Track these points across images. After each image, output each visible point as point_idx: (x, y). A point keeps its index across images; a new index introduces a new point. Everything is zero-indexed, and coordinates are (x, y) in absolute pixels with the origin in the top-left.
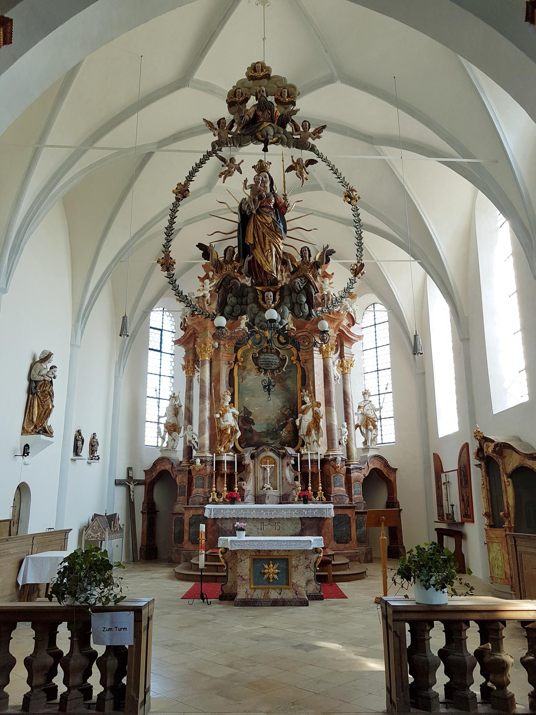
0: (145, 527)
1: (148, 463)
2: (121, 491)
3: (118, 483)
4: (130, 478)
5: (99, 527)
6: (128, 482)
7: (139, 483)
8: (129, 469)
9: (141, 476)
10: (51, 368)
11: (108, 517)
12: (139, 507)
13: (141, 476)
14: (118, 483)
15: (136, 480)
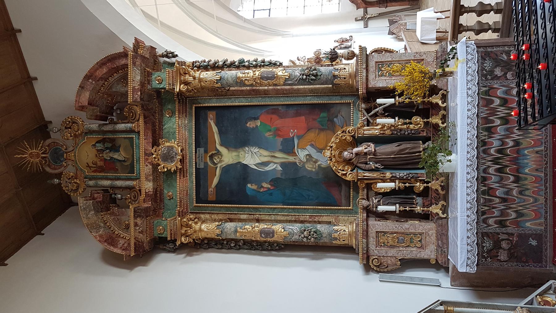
0: (397, 4)
1: (352, 7)
2: (371, 23)
3: (366, 26)
4: (362, 19)
5: (397, 28)
6: (365, 20)
7: (366, 12)
8: (356, 20)
9: (361, 11)
10: (299, 60)
11: (390, 25)
12: (383, 10)
13: (361, 11)
14: (366, 26)
15: (364, 14)
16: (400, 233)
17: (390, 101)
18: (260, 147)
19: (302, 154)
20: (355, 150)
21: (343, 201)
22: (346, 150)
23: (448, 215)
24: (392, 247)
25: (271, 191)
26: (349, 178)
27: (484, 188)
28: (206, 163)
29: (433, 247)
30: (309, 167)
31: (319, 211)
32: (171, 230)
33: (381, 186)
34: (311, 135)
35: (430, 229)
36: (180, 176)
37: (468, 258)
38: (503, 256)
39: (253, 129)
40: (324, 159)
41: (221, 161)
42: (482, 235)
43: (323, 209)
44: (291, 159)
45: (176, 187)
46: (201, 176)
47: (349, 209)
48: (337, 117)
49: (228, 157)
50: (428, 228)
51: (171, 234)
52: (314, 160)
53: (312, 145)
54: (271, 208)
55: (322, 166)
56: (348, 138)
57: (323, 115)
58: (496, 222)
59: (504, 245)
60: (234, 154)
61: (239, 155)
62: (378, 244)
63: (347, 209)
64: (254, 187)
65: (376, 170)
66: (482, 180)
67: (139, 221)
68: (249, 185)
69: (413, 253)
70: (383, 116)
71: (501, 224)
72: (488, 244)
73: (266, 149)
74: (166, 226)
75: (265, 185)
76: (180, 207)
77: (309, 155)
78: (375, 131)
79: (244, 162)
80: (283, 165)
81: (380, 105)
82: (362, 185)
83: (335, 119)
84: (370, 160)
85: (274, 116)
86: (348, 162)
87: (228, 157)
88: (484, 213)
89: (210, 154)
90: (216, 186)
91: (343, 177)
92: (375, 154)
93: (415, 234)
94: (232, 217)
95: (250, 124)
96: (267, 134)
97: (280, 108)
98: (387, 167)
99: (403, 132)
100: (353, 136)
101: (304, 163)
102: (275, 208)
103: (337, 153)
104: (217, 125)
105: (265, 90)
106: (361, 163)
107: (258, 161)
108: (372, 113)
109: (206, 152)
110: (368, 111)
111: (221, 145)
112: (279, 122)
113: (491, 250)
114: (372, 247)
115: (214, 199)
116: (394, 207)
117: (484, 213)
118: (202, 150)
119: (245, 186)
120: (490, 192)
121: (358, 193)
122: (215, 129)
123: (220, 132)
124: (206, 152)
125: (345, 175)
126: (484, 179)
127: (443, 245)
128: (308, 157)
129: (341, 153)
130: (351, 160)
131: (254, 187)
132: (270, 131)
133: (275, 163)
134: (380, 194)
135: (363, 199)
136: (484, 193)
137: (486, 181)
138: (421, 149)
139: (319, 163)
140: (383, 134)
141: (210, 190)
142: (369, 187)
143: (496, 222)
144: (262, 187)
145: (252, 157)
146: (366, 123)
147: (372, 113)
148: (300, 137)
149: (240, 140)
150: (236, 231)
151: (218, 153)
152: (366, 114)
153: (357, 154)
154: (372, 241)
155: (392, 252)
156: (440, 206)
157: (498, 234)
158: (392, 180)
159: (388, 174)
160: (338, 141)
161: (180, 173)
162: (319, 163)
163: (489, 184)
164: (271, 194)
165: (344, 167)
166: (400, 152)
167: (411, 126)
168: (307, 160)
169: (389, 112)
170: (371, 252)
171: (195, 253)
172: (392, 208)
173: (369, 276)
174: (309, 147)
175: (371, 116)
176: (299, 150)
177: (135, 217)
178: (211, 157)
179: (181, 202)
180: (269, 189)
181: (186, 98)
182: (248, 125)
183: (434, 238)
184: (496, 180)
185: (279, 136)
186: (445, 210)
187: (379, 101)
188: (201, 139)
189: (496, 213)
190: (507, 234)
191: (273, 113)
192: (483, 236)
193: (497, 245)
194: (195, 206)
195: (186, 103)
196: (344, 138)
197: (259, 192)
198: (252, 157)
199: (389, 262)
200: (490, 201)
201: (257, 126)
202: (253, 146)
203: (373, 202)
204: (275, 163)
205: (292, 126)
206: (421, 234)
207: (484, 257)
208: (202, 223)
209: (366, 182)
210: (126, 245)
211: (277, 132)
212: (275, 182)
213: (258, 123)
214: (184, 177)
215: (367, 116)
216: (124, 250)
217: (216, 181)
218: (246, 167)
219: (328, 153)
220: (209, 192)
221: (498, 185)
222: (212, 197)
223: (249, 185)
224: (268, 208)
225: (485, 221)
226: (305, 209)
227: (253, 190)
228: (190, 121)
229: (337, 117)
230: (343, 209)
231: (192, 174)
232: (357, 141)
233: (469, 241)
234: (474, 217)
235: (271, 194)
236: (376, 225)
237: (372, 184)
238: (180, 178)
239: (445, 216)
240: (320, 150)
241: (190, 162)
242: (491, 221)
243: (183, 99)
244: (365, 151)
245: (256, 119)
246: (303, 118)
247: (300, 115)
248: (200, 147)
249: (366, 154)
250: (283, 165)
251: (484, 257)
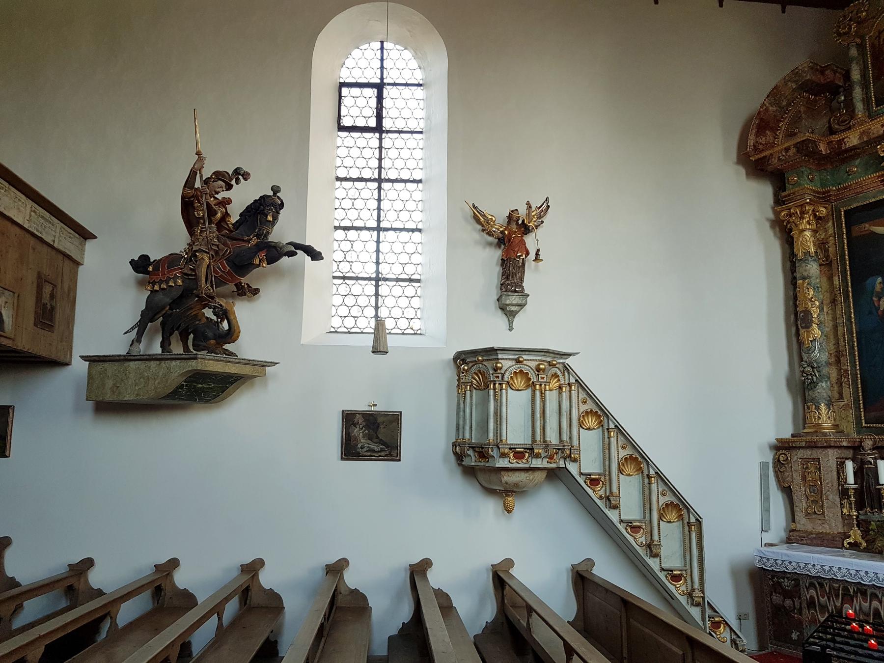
16: (821, 488)
23: (847, 549)
24: (804, 478)
27: (852, 591)
29: (809, 527)
31: (855, 381)
32: (794, 193)
35: (830, 525)
37: (768, 559)
38: (777, 598)
42: (796, 578)
50: (833, 525)
51: (789, 195)
58: (812, 597)
59: (788, 602)
62: (806, 461)
64: (878, 287)
66: (862, 590)
67: (793, 151)
68: (880, 279)
69: (802, 504)
71: (811, 604)
72: (787, 584)
74: (800, 185)
88: (821, 585)
93: (822, 506)
94: (834, 265)
113: (781, 587)
114: (801, 453)
115: (854, 234)
116: (853, 482)
117: (821, 585)
119: (878, 275)
120: (848, 598)
126: (864, 593)
127: (809, 539)
131: (878, 287)
135: (875, 442)
136: (846, 589)
137: (861, 594)
141: (867, 225)
143: (812, 597)
150: (804, 278)
154: (808, 453)
155: (797, 478)
156: (860, 539)
157: (800, 598)
163: (857, 597)
164: (870, 313)
170: (794, 452)
171: (778, 229)
172: (851, 479)
173: (768, 449)
177: (795, 145)
183: (820, 529)
184: (863, 608)
186: (854, 546)
189: (823, 600)
190: (801, 607)
192: (794, 580)
193: (787, 594)
199: (786, 474)
200: (837, 596)
203: (868, 455)
206: (823, 513)
207: (773, 577)
208: (812, 230)
210: (761, 147)
216: (754, 146)
220: (863, 225)
221: (858, 608)
222: (857, 230)
223: (880, 279)
225: (812, 585)
227: (874, 287)
233: (787, 563)
234: (814, 573)
235: (870, 313)
236: (830, 459)
239: (846, 545)
242: (812, 592)
251: (773, 577)
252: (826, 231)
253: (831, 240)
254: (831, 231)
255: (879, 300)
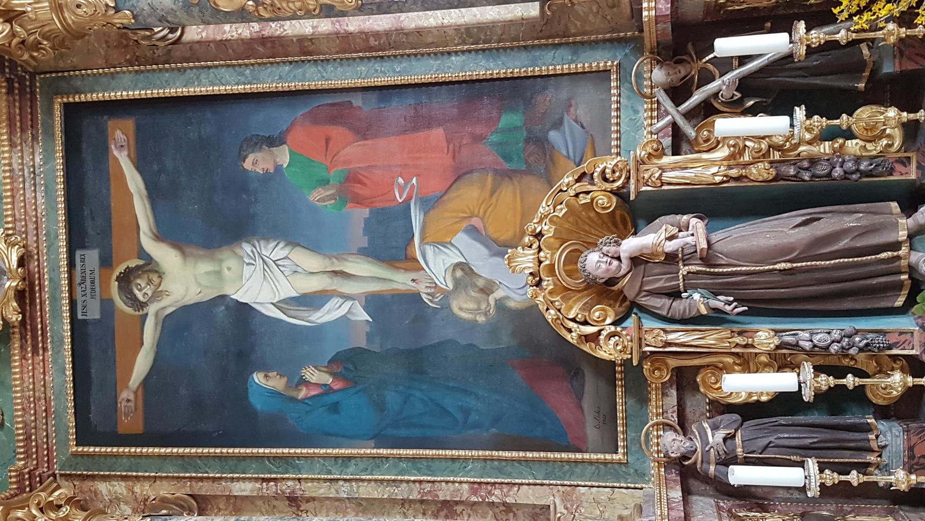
17: (769, 44)
18: (293, 243)
19: (438, 265)
20: (631, 245)
21: (592, 433)
22: (592, 245)
25: (333, 398)
26: (607, 351)
28: (107, 305)
30: (464, 307)
33: (739, 385)
34: (469, 194)
36: (23, 348)
39: (267, 178)
40: (513, 279)
41: (157, 295)
43: (519, 461)
44: (401, 281)
45: (9, 388)
46: (93, 348)
47: (612, 462)
48: (558, 125)
49: (184, 279)
52: (480, 283)
53: (473, 232)
54: (336, 458)
55: (511, 304)
56: (602, 200)
57: (510, 119)
60: (204, 267)
61: (218, 273)
63: (605, 463)
64: (276, 383)
65: (716, 318)
70: (737, 108)
73: (314, 247)
75: (315, 376)
76: (28, 455)
77: (464, 267)
78: (705, 169)
79: (241, 296)
80: (374, 303)
81: (725, 64)
82: (658, 377)
83: (553, 135)
84: (691, 282)
85: (338, 132)
86: (605, 290)
87: (184, 279)
89: (121, 268)
90: (146, 382)
91: (586, 348)
92: (708, 258)
94: (204, 489)
95: (257, 162)
96: (315, 196)
97: (357, 101)
98: (761, 308)
99: (821, 169)
100: (620, 194)
101: (447, 295)
102: (350, 458)
103: (559, 257)
104: (140, 165)
105: (302, 39)
106: (651, 293)
107: (287, 291)
108: (697, 97)
109: (106, 262)
110: (678, 93)
111: (160, 236)
112: (353, 152)
115: (139, 428)
118: (91, 257)
121: (644, 401)
122: (134, 181)
123: (154, 193)
124: (106, 262)
125: (593, 338)
128: (459, 273)
129: (574, 258)
130: (612, 281)
131: (276, 383)
132: (324, 183)
133: (347, 297)
134: (730, 408)
135: (667, 426)
138: (902, 235)
139: (499, 294)
140: (737, 179)
142: (685, 380)
144: (304, 382)
145: (264, 278)
146: (667, 142)
147: (697, 97)
148: (429, 204)
149: (223, 217)
151: (149, 266)
152: (668, 104)
153: (636, 261)
158: (782, 360)
159: (765, 336)
160: (562, 211)
161: (23, 337)
162: (499, 294)
164: (335, 408)
165: (588, 307)
166: (811, 249)
167: (853, 146)
168: (457, 283)
169: (766, 90)
174: (462, 239)
175: (689, 115)
176: (429, 250)
178: (126, 279)
179: (28, 438)
180: (327, 390)
181: (33, 76)
182: (248, 165)
185: (359, 201)
187: (725, 46)
188: (87, 215)
191: (333, 120)
194: (75, 455)
195: (33, 93)
196: (584, 200)
197: (293, 400)
198: (264, 278)
201: (278, 168)
202: (267, 239)
203: (705, 442)
204: (347, 297)
205: (401, 161)
209: (673, 363)
211: (351, 188)
212: (348, 363)
213: (283, 155)
214: (35, 351)
215: (674, 113)
217: (142, 364)
218: (243, 313)
219: (526, 259)
220: (122, 405)
222: (129, 417)
224: (325, 457)
226: (453, 459)
227: (274, 394)
228: (48, 156)
229: (558, 125)
230: (591, 463)
231: (62, 343)
232: (634, 212)
235: (335, 408)
237: (698, 369)
238: (24, 357)
240: (501, 247)
241: (55, 299)
243: (21, 80)
244: (670, 246)
245: (273, 142)
246: (438, 134)
247: (429, 123)
248: (83, 247)
249: (671, 258)
250: (374, 303)
252: (116, 500)
253: (144, 489)
254: (120, 488)
255: (307, 383)
